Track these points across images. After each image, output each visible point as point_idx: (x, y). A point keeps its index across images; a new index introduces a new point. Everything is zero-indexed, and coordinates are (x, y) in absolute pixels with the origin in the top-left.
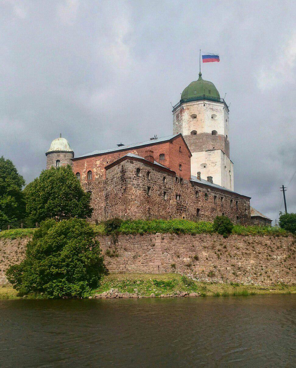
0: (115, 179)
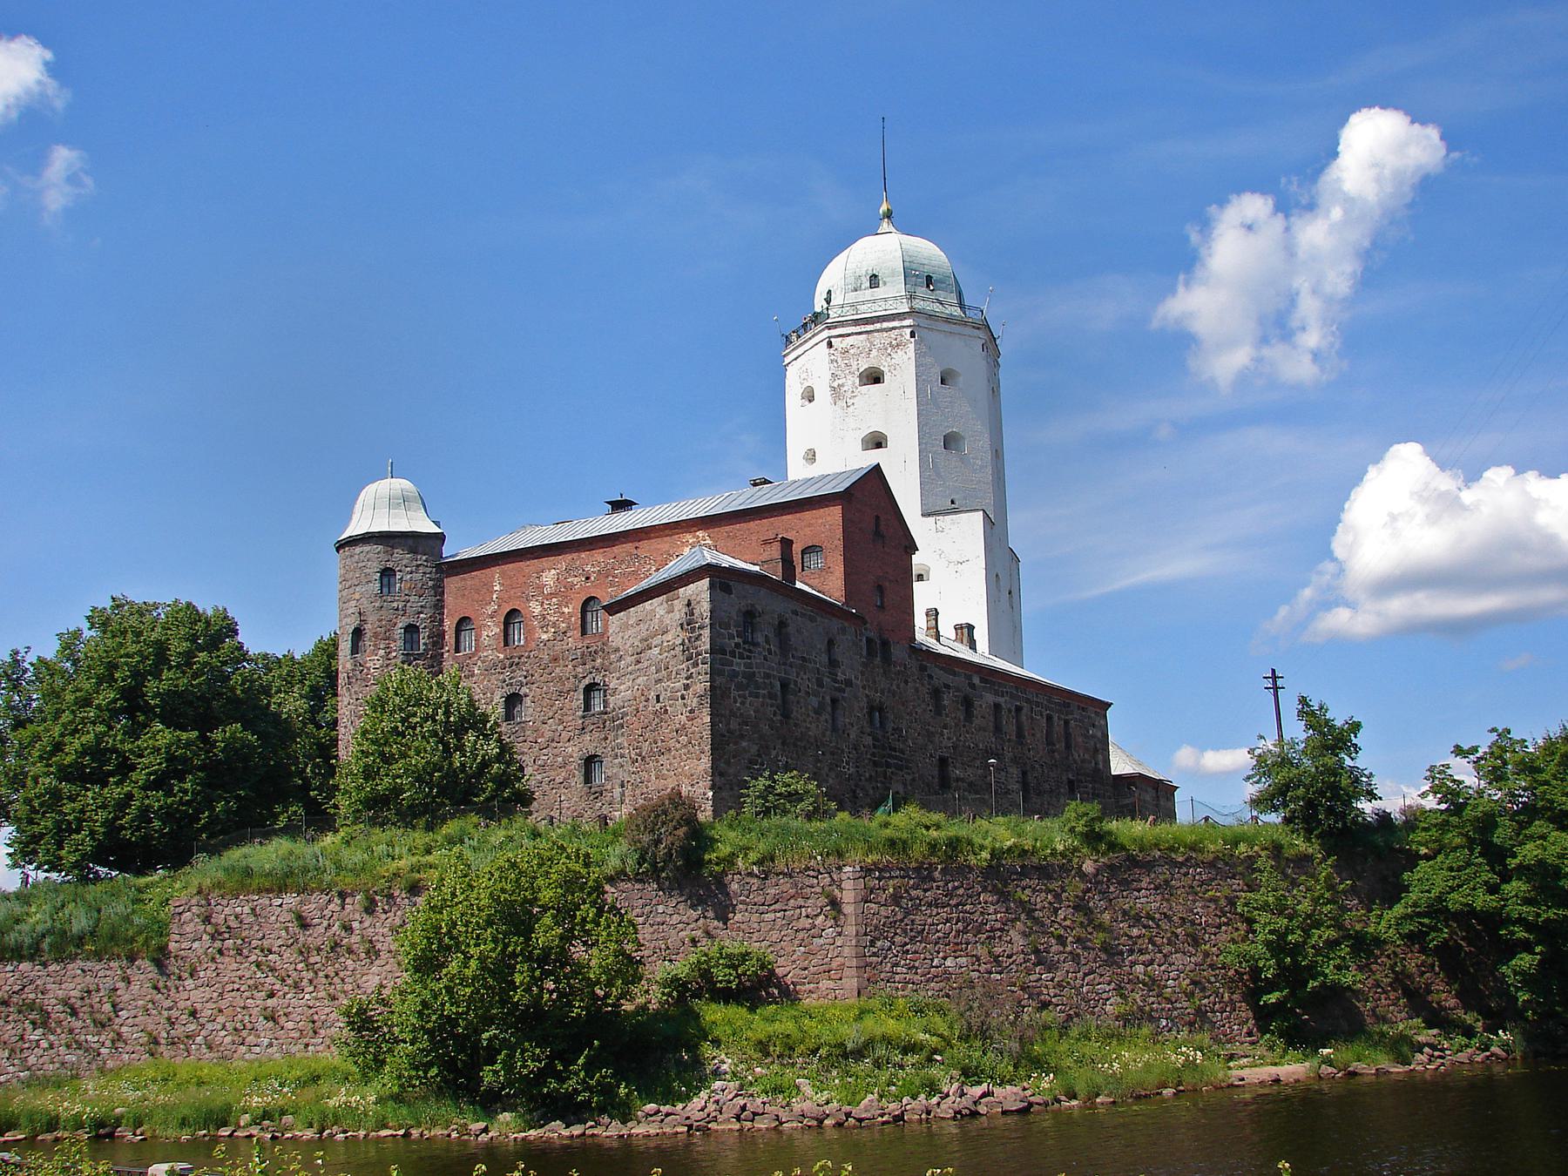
0: (656, 651)
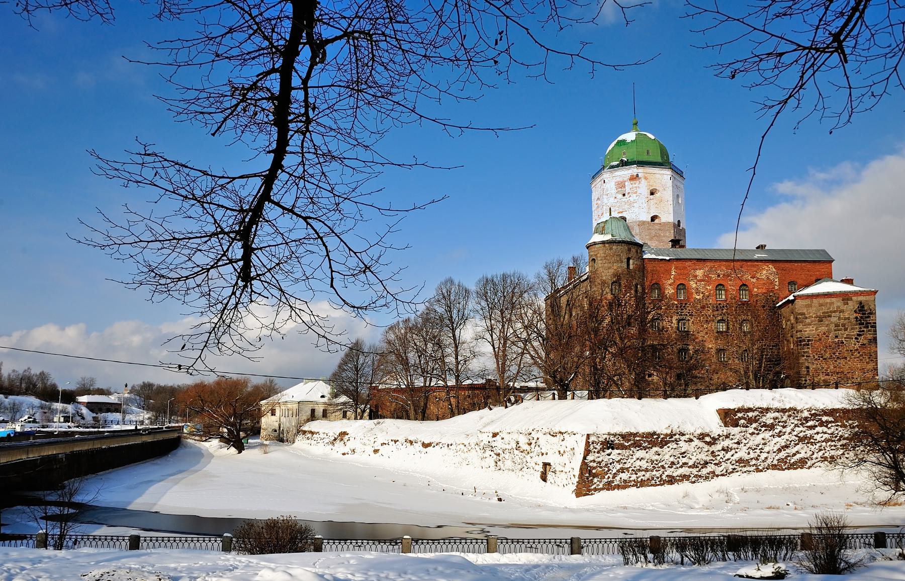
0: (834, 319)
